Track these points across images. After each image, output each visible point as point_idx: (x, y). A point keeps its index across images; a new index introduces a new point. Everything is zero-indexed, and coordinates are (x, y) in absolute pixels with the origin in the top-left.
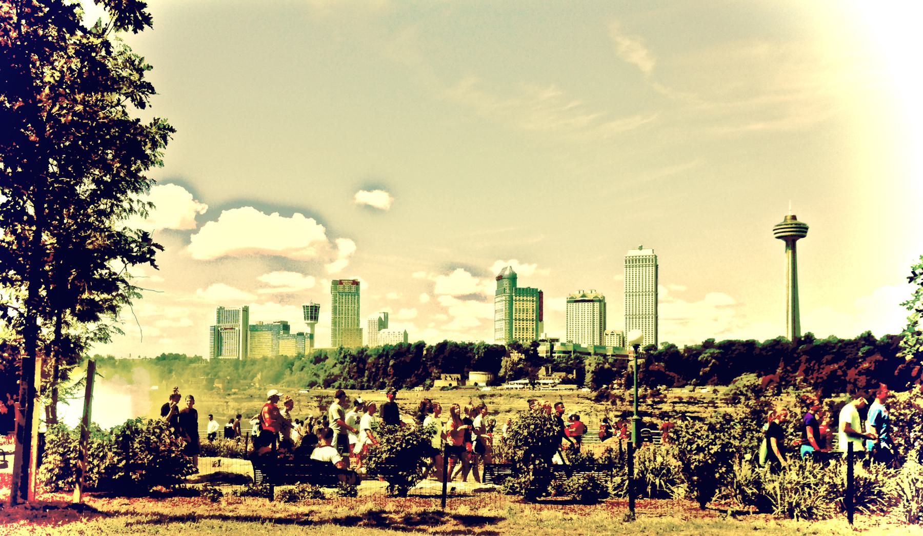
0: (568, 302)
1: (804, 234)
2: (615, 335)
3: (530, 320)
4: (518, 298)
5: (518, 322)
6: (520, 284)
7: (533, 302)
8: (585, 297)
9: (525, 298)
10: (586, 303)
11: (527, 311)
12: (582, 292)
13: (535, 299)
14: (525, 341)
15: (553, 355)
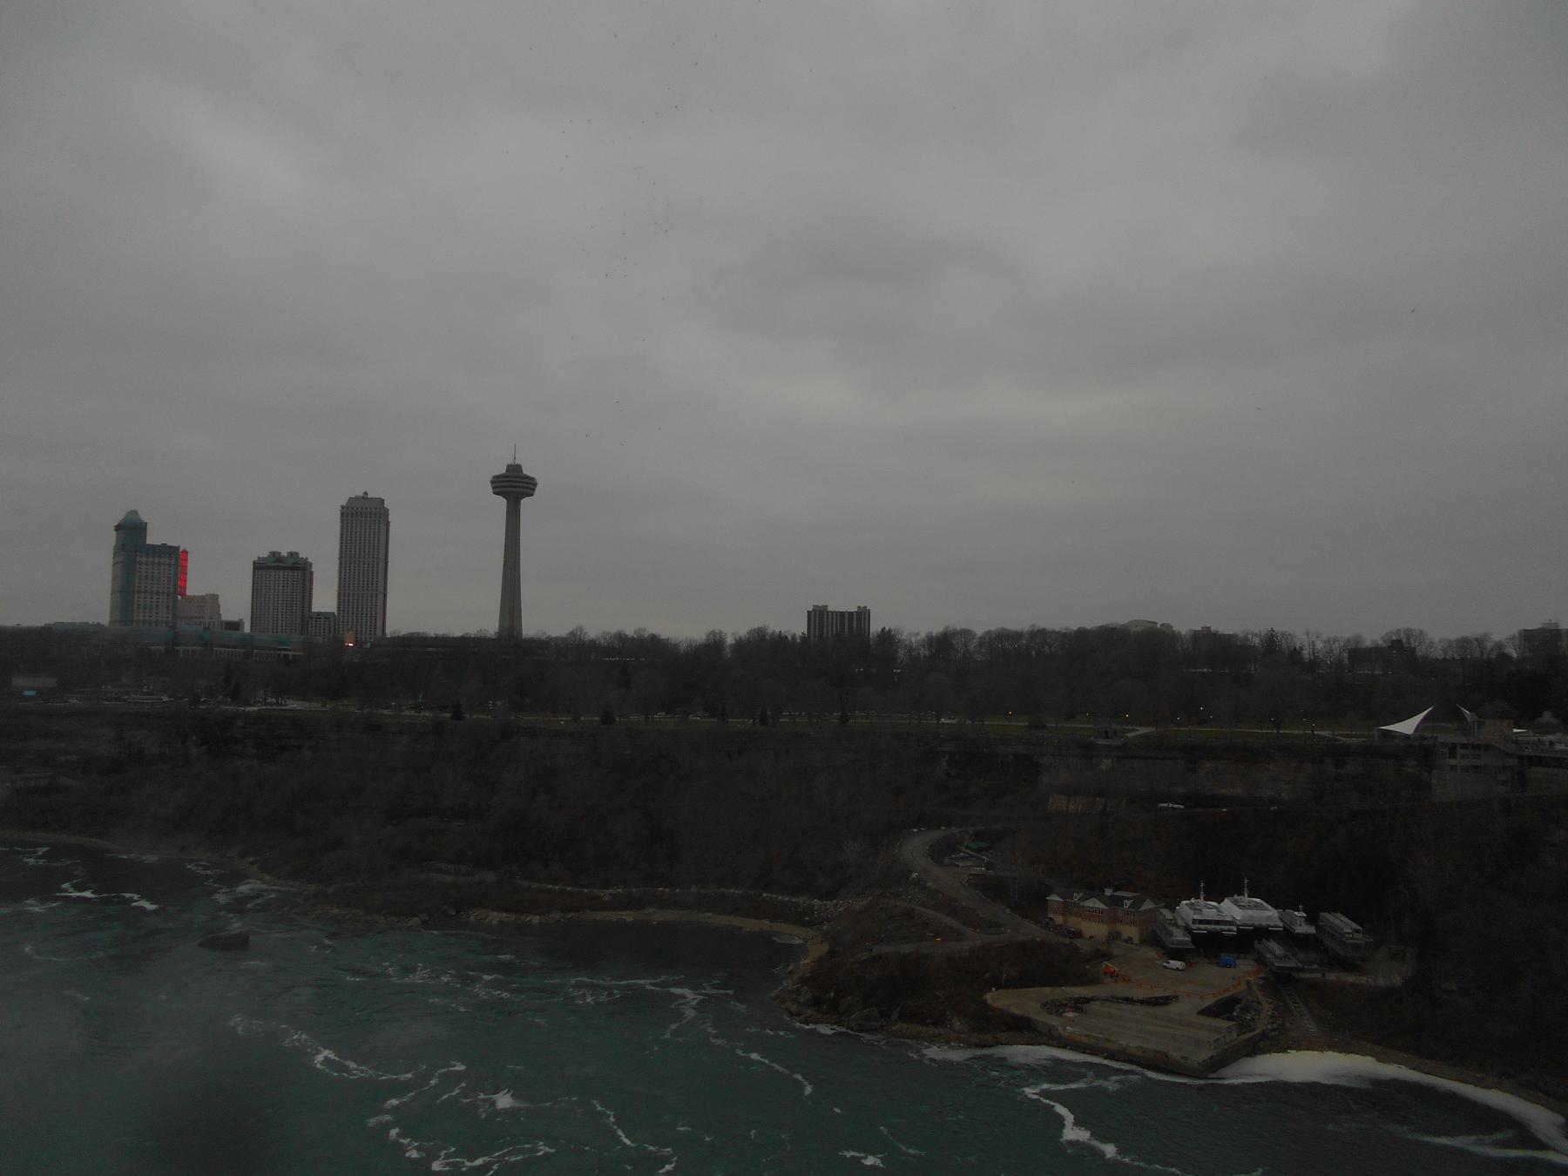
0: (255, 568)
1: (531, 491)
2: (322, 620)
3: (163, 593)
4: (144, 560)
5: (142, 595)
6: (153, 538)
7: (169, 565)
8: (281, 562)
9: (156, 560)
10: (281, 573)
11: (159, 580)
12: (277, 555)
13: (173, 562)
14: (154, 624)
15: (177, 648)
